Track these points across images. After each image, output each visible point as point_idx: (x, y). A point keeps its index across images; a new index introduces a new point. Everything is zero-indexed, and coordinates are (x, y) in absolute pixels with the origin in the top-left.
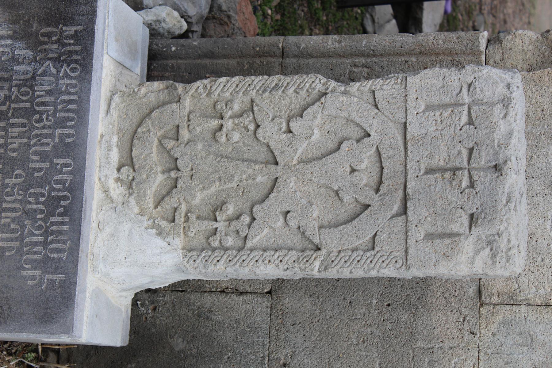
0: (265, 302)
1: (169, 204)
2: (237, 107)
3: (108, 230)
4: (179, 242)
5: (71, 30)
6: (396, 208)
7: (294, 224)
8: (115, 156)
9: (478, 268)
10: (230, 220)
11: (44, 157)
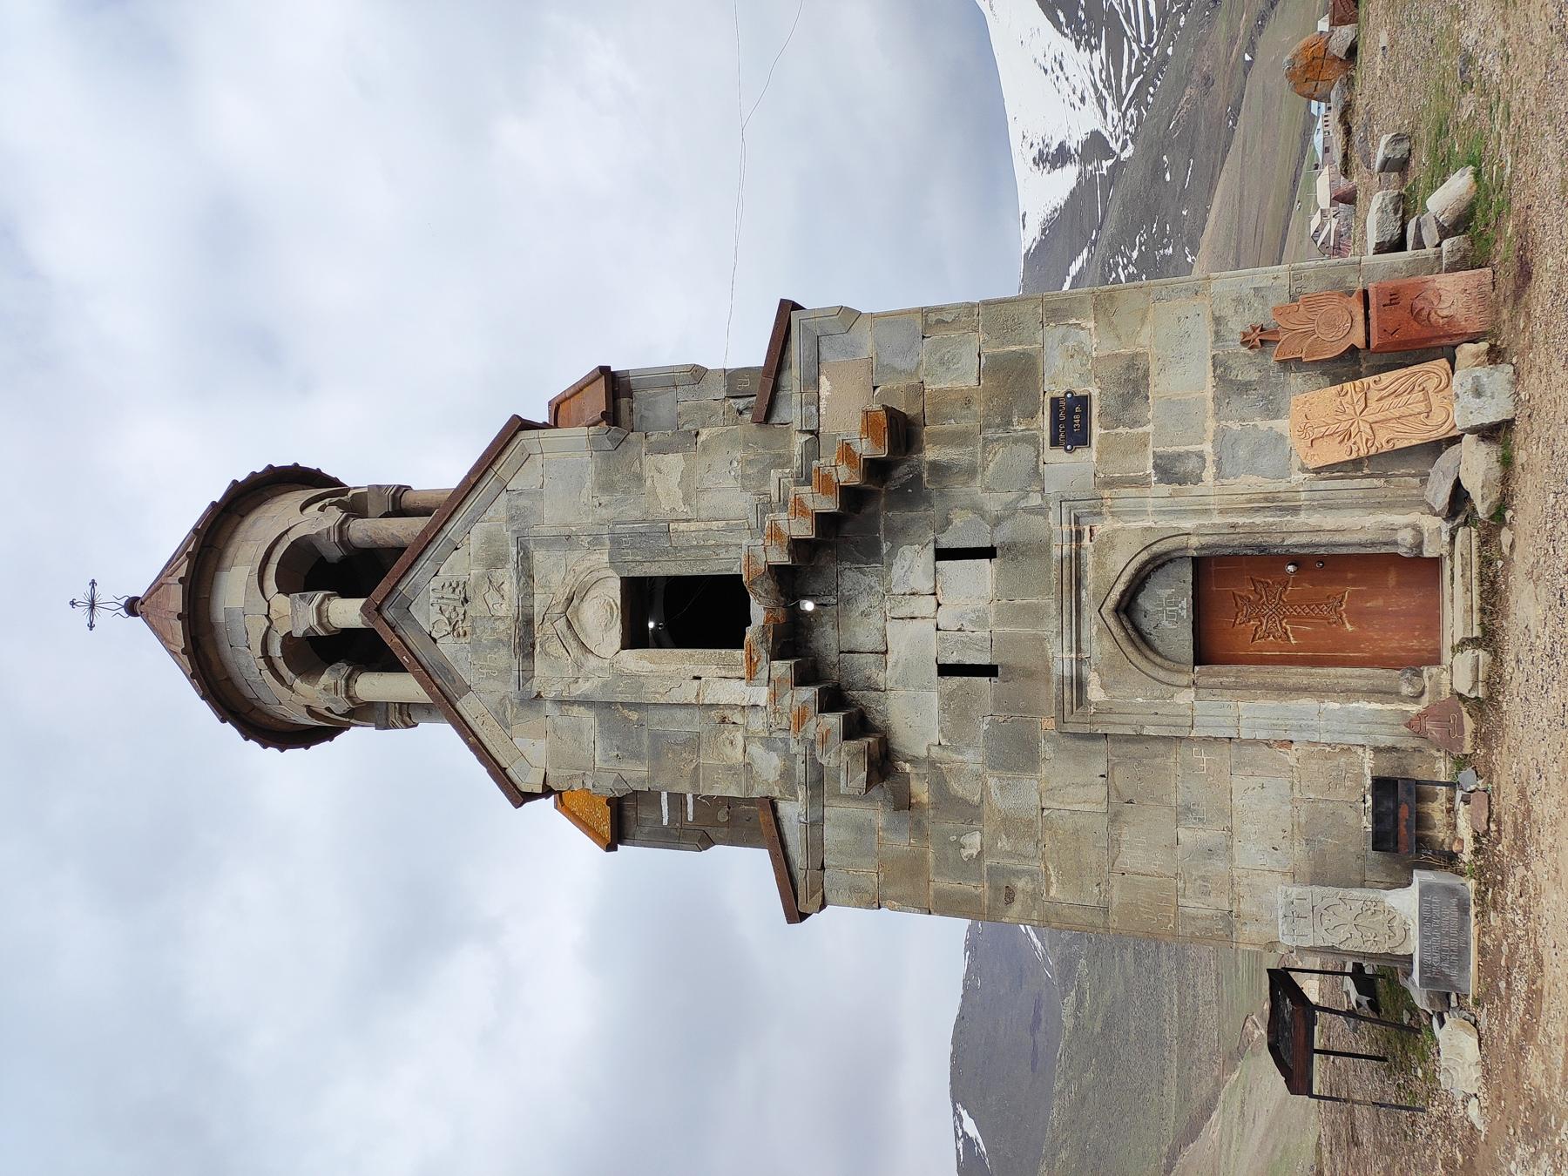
0: (1366, 878)
1: (1391, 916)
2: (1369, 942)
3: (1412, 910)
4: (1386, 904)
5: (1429, 975)
6: (1315, 908)
7: (1348, 906)
8: (1411, 933)
9: (1290, 889)
10: (1370, 909)
11: (1435, 936)
